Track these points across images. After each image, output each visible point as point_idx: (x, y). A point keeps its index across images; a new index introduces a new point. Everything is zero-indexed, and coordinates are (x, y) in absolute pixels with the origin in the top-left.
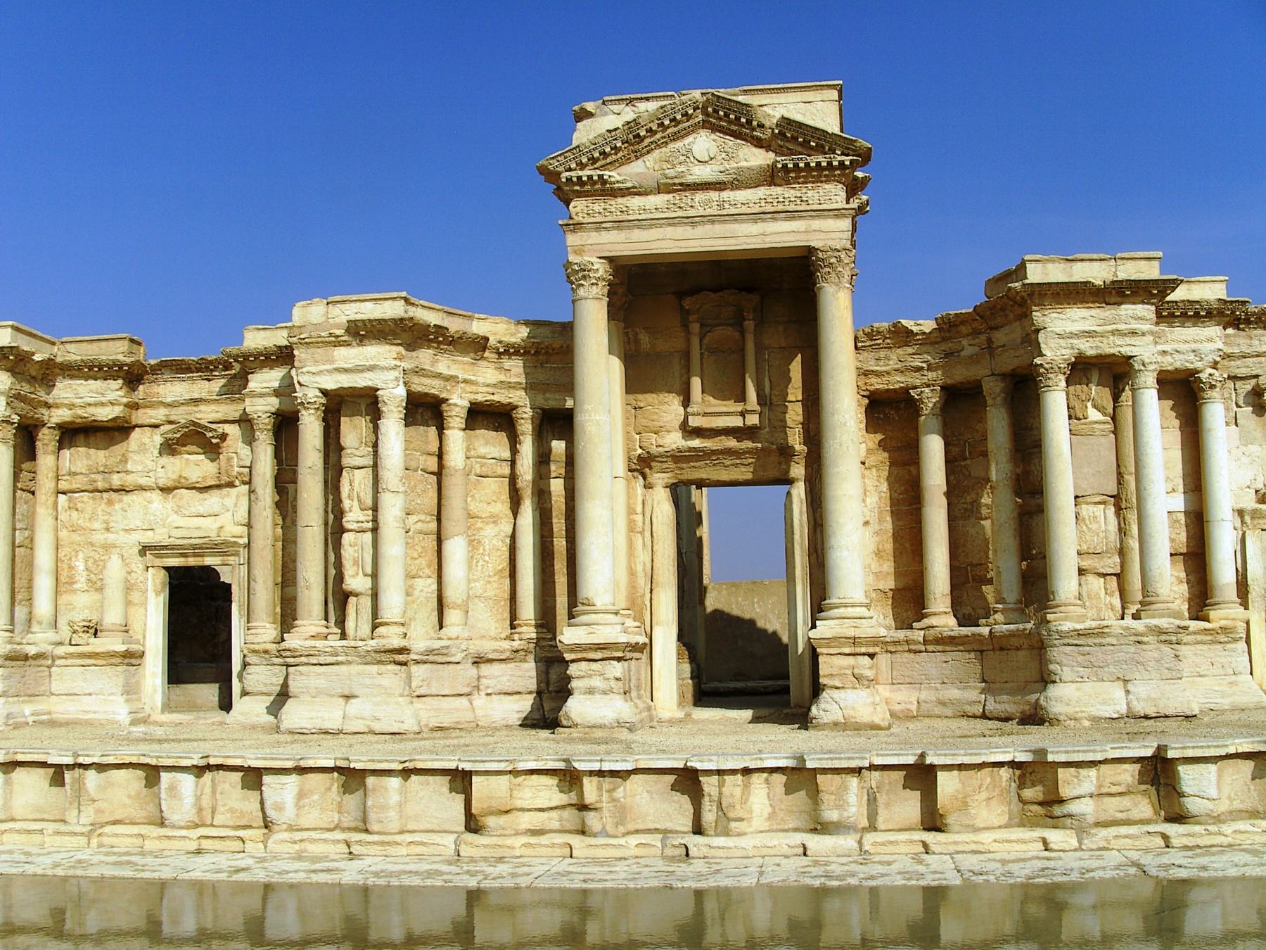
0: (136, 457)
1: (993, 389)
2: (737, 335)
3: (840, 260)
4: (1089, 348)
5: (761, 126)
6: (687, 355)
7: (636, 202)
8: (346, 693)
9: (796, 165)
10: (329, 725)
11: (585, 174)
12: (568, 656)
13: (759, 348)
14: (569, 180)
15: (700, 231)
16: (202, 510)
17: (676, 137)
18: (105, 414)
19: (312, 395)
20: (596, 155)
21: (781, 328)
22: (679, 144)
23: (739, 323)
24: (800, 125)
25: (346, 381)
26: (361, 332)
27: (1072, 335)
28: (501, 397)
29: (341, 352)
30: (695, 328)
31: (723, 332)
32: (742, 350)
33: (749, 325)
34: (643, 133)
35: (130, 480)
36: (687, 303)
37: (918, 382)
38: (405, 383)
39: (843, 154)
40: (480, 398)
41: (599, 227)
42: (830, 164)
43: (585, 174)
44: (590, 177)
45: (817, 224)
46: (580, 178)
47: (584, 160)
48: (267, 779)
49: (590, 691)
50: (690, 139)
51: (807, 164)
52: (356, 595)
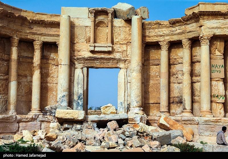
27: (213, 28)
40: (23, 37)
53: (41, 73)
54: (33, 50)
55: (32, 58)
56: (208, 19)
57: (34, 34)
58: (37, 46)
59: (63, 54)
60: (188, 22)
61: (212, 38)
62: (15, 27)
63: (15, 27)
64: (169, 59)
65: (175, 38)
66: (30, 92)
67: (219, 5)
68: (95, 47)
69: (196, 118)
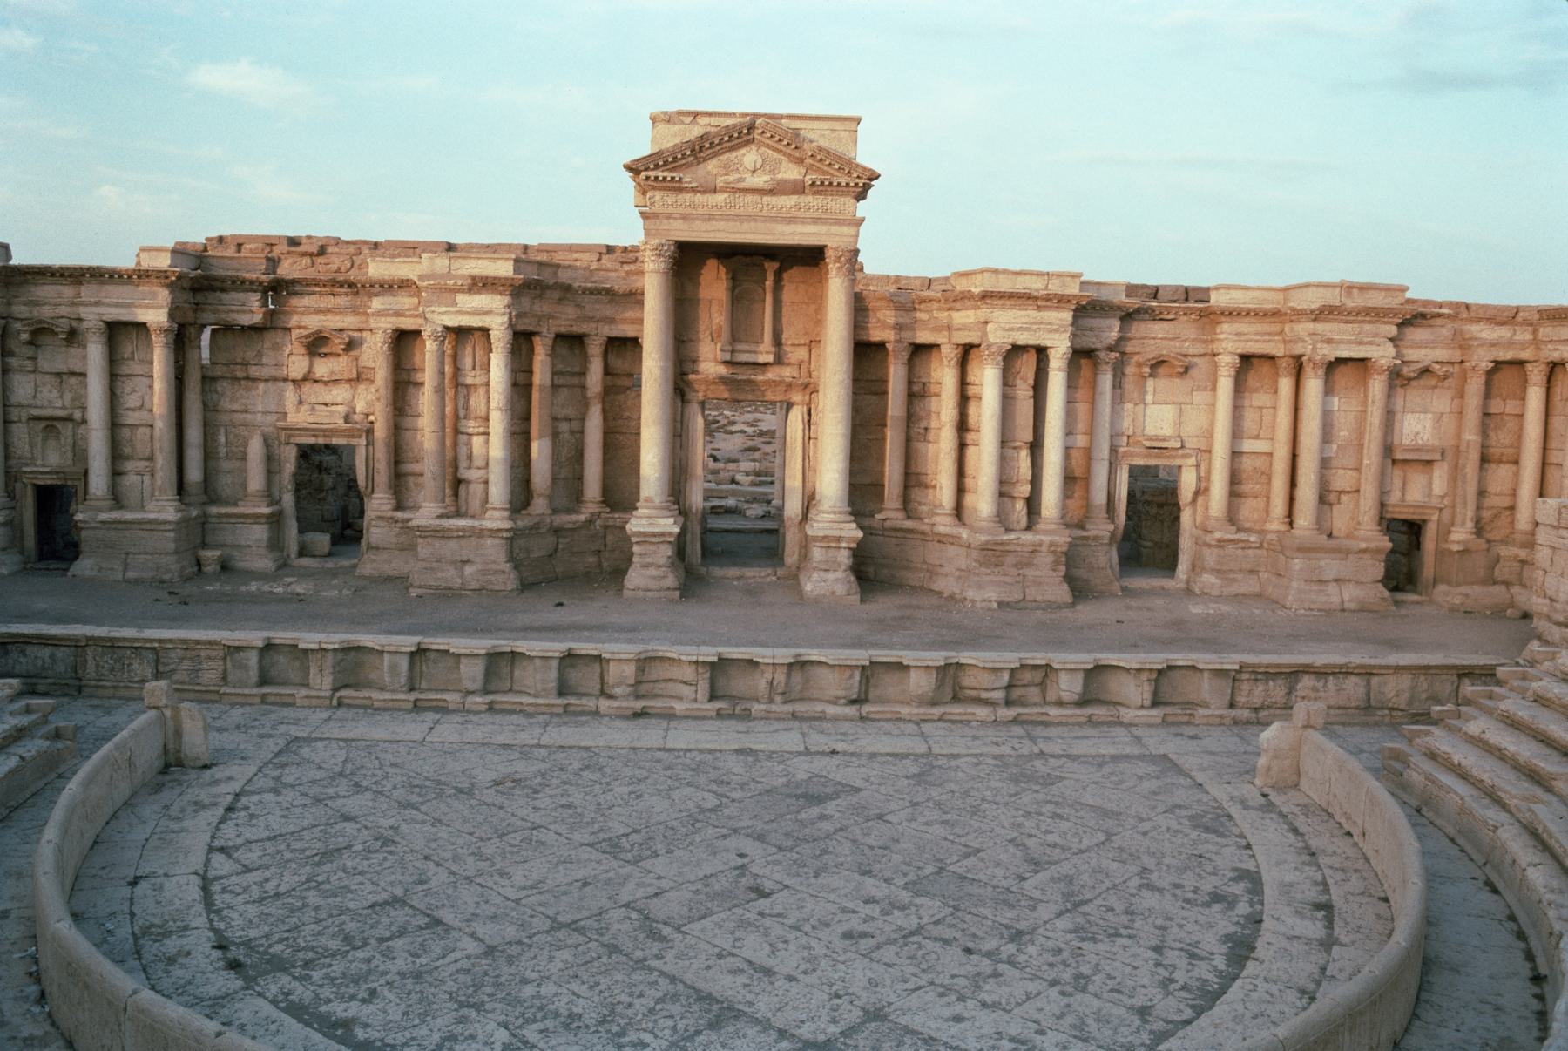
0: (270, 353)
1: (949, 353)
4: (1023, 339)
11: (661, 174)
12: (634, 539)
15: (746, 226)
16: (328, 400)
17: (732, 149)
18: (246, 320)
22: (734, 154)
25: (465, 321)
26: (481, 284)
29: (460, 298)
35: (266, 372)
40: (563, 330)
41: (669, 216)
43: (661, 174)
45: (835, 229)
46: (656, 178)
48: (463, 660)
50: (743, 151)
52: (468, 482)
53: (604, 411)
54: (585, 359)
55: (583, 373)
56: (1003, 307)
57: (591, 319)
58: (595, 349)
59: (653, 367)
60: (958, 305)
61: (1009, 352)
62: (546, 309)
63: (546, 309)
64: (910, 383)
66: (579, 456)
67: (1027, 277)
68: (733, 352)
69: (965, 533)
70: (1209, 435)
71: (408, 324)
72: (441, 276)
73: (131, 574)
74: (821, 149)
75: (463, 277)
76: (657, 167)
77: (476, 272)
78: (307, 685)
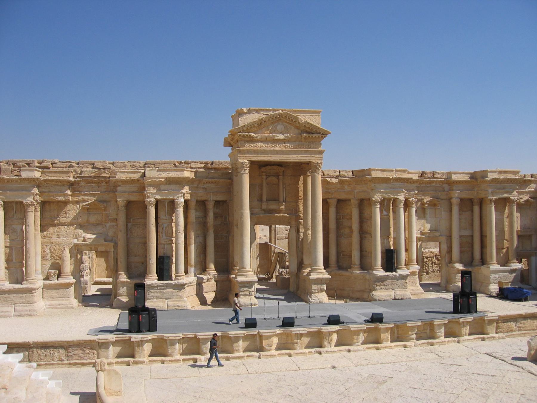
1: (354, 203)
2: (276, 180)
3: (319, 166)
5: (299, 123)
6: (261, 185)
7: (259, 144)
8: (167, 297)
9: (309, 137)
10: (162, 309)
13: (283, 184)
14: (240, 135)
19: (153, 200)
20: (249, 128)
21: (289, 178)
23: (277, 176)
24: (311, 124)
28: (203, 198)
30: (264, 177)
31: (273, 179)
32: (279, 184)
33: (281, 177)
34: (263, 122)
36: (263, 169)
37: (330, 197)
38: (184, 198)
39: (323, 134)
42: (319, 137)
44: (247, 135)
46: (244, 135)
47: (245, 129)
49: (245, 295)
50: (276, 124)
51: (312, 136)
53: (214, 232)
58: (211, 206)
64: (337, 215)
65: (343, 196)
70: (450, 230)
71: (133, 198)
72: (155, 178)
73: (17, 313)
74: (308, 123)
75: (162, 178)
76: (244, 131)
77: (169, 176)
78: (133, 357)
